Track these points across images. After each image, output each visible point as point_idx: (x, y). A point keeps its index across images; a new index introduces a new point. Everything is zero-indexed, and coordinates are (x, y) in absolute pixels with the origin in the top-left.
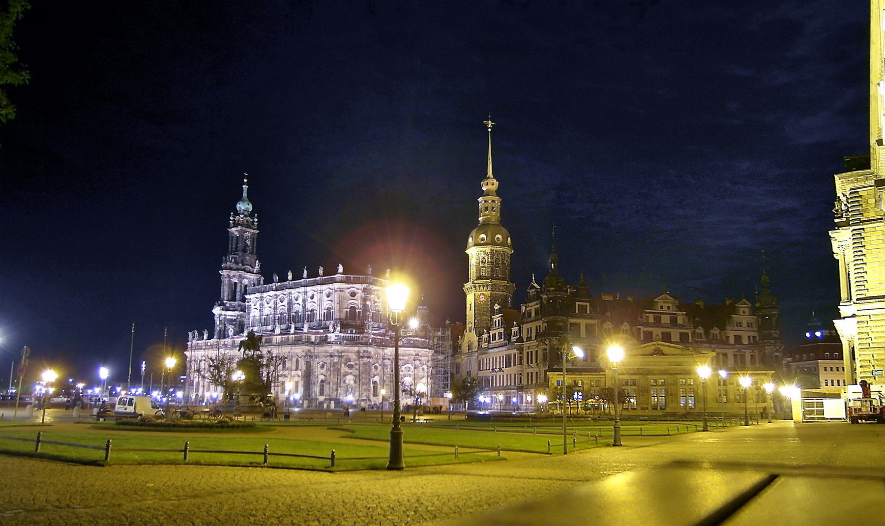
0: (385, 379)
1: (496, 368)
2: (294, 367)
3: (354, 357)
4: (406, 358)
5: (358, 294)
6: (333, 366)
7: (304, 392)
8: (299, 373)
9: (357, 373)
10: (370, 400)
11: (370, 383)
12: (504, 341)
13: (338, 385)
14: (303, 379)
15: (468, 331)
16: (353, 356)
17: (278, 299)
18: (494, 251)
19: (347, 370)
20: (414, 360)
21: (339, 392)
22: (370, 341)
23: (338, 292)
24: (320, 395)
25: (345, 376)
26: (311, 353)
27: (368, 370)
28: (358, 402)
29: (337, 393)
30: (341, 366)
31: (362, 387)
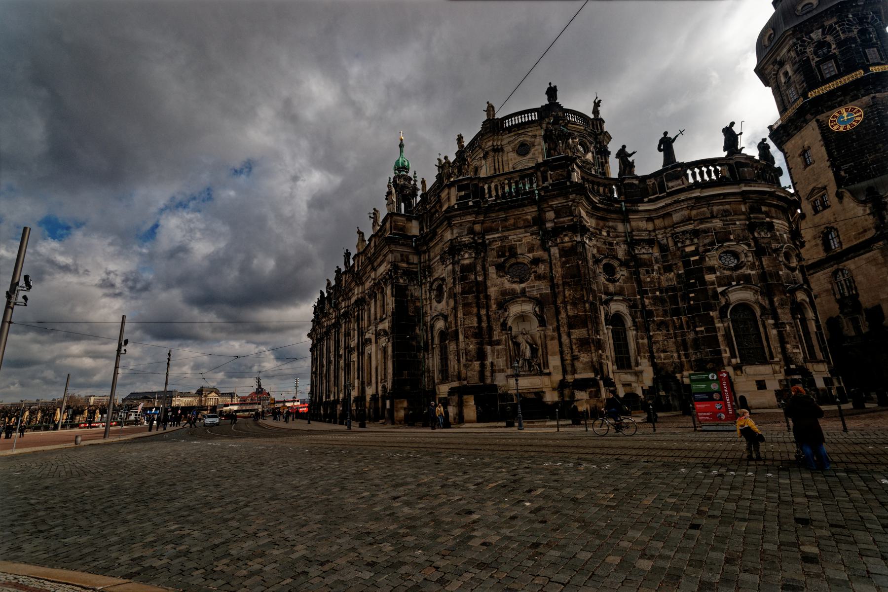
0: (650, 307)
4: (717, 223)
5: (534, 146)
8: (385, 325)
9: (544, 287)
10: (609, 383)
11: (597, 318)
13: (483, 336)
20: (752, 227)
21: (488, 363)
23: (492, 154)
24: (443, 379)
25: (503, 306)
28: (561, 395)
29: (483, 366)
30: (486, 275)
31: (569, 335)
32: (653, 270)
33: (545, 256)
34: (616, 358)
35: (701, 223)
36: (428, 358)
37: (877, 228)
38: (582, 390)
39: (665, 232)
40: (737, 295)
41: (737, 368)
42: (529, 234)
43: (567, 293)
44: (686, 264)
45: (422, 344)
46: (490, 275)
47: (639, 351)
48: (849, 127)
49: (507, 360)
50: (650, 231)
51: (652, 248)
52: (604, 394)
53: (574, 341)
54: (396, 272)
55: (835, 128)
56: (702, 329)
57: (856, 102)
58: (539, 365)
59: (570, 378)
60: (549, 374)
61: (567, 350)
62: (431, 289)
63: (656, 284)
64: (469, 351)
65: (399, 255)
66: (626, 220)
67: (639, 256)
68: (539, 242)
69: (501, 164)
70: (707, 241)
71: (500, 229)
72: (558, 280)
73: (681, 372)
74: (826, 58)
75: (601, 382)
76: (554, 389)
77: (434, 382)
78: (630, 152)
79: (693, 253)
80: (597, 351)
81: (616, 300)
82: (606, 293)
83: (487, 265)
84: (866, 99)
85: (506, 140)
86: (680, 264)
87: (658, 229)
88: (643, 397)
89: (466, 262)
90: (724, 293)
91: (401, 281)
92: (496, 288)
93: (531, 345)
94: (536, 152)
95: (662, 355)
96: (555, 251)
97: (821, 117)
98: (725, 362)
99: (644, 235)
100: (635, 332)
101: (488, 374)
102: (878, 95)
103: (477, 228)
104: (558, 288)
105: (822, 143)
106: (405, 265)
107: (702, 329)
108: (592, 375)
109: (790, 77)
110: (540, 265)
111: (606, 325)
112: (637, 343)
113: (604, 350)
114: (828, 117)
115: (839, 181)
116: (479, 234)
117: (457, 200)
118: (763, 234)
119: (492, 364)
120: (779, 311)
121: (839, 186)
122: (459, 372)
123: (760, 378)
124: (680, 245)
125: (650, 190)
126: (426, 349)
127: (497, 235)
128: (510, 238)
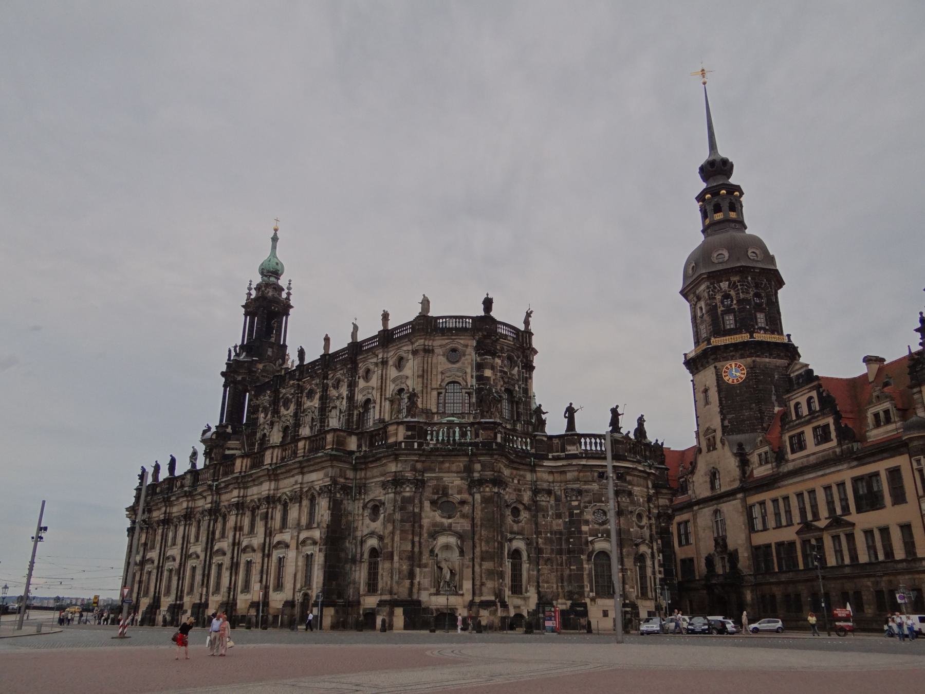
0: (541, 546)
1: (819, 520)
2: (304, 521)
3: (458, 482)
5: (464, 355)
6: (402, 509)
7: (324, 584)
8: (317, 534)
10: (504, 606)
11: (502, 553)
12: (840, 444)
13: (414, 559)
14: (324, 547)
15: (704, 449)
16: (454, 481)
17: (304, 394)
18: (750, 278)
19: (437, 517)
22: (499, 440)
23: (422, 354)
24: (369, 591)
25: (433, 535)
26: (346, 479)
27: (497, 516)
29: (412, 584)
30: (421, 508)
31: (481, 565)
32: (548, 515)
33: (470, 499)
34: (512, 585)
35: (585, 485)
36: (355, 571)
37: (741, 481)
38: (485, 609)
39: (560, 486)
40: (600, 545)
41: (593, 600)
42: (459, 479)
43: (483, 533)
44: (571, 515)
45: (350, 557)
46: (425, 508)
47: (529, 582)
48: (735, 381)
49: (431, 581)
50: (550, 482)
51: (550, 497)
52: (500, 613)
53: (483, 570)
54: (335, 488)
55: (726, 379)
56: (574, 567)
57: (742, 360)
58: (455, 587)
59: (477, 600)
60: (462, 595)
61: (477, 577)
62: (365, 507)
63: (549, 528)
64: (403, 571)
65: (338, 470)
66: (533, 470)
67: (539, 503)
68: (466, 487)
69: (430, 365)
70: (587, 499)
71: (437, 470)
72: (478, 521)
73: (557, 600)
74: (728, 310)
75: (499, 604)
76: (465, 607)
77: (359, 593)
78: (544, 411)
79: (578, 507)
80: (498, 580)
81: (517, 539)
82: (511, 533)
83: (423, 499)
84: (749, 360)
85: (438, 342)
86: (567, 514)
87: (557, 482)
88: (527, 617)
89: (407, 494)
90: (592, 542)
91: (338, 495)
92: (429, 520)
93: (451, 571)
94: (466, 362)
95: (546, 585)
96: (478, 497)
97: (719, 365)
98: (586, 594)
99: (545, 486)
100: (528, 565)
101: (415, 590)
102: (758, 359)
103: (419, 466)
104: (477, 527)
105: (716, 389)
106: (342, 480)
107: (574, 567)
108: (493, 598)
109: (703, 315)
110: (465, 506)
111: (508, 558)
112: (529, 574)
113: (503, 580)
114: (723, 366)
115: (724, 428)
116: (420, 471)
117: (404, 438)
118: (624, 499)
119: (419, 582)
120: (625, 560)
121: (723, 434)
122: (391, 588)
123: (605, 608)
124: (568, 498)
125: (554, 448)
126: (354, 561)
127: (434, 475)
128: (444, 479)
